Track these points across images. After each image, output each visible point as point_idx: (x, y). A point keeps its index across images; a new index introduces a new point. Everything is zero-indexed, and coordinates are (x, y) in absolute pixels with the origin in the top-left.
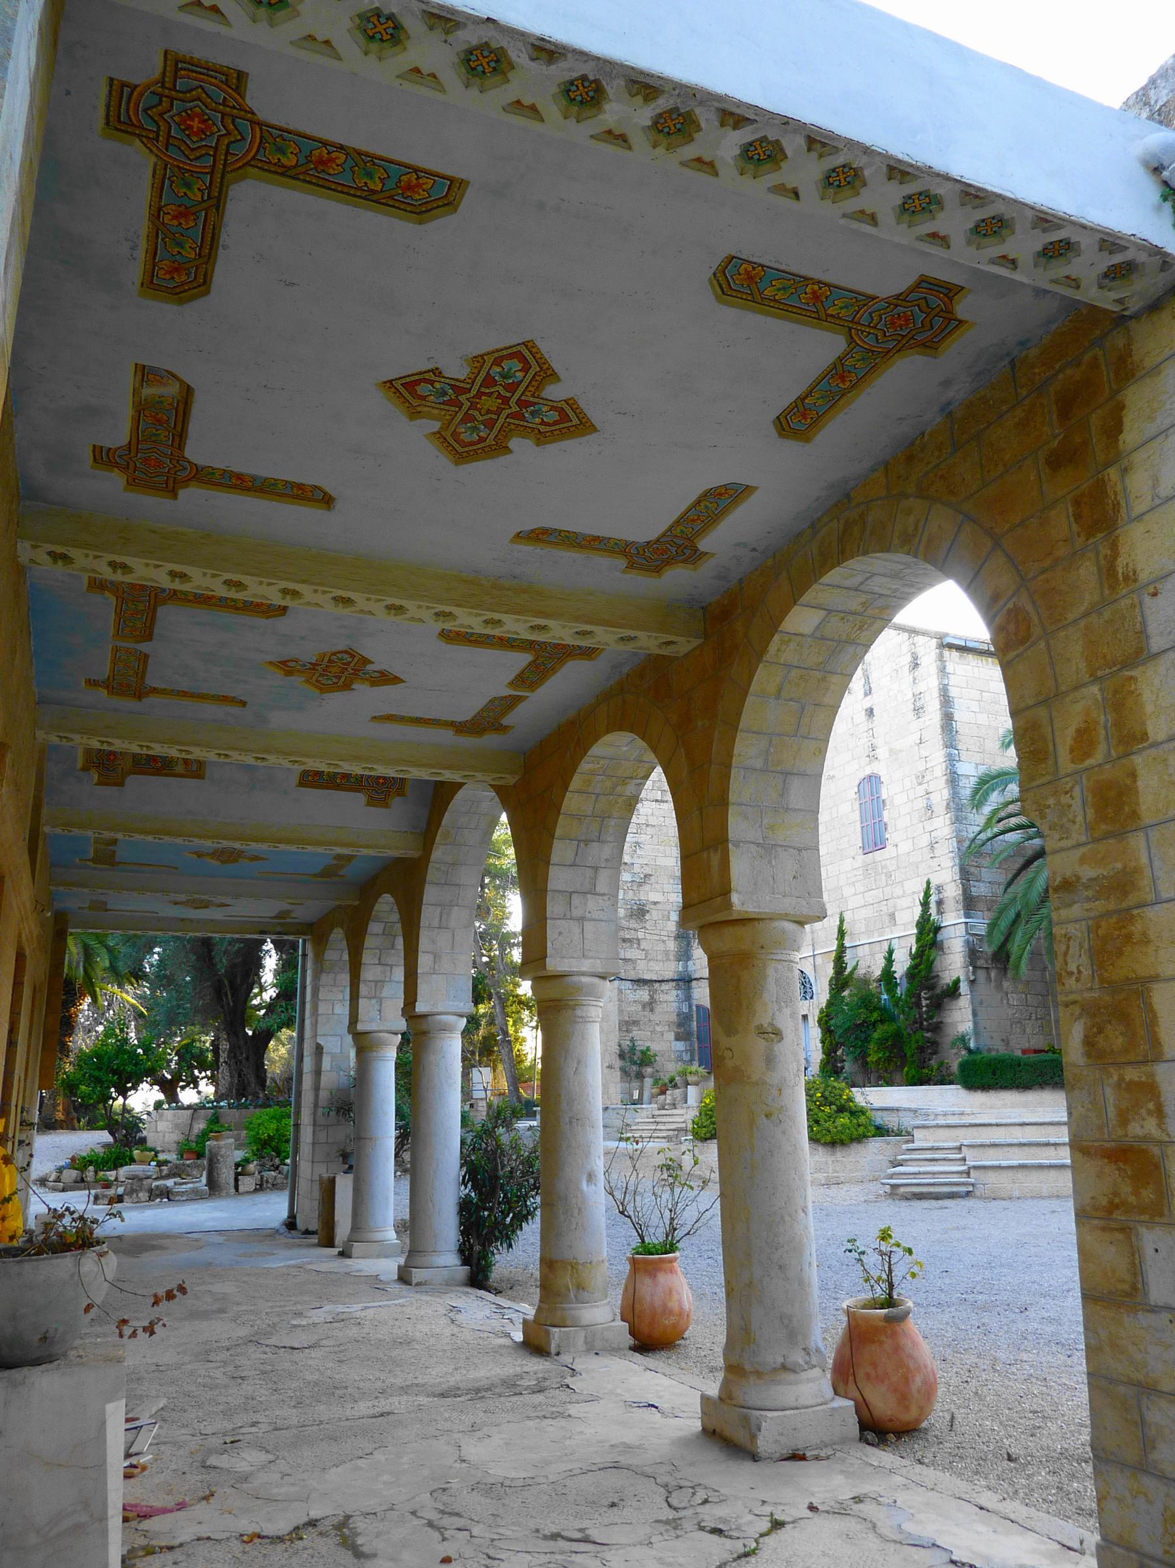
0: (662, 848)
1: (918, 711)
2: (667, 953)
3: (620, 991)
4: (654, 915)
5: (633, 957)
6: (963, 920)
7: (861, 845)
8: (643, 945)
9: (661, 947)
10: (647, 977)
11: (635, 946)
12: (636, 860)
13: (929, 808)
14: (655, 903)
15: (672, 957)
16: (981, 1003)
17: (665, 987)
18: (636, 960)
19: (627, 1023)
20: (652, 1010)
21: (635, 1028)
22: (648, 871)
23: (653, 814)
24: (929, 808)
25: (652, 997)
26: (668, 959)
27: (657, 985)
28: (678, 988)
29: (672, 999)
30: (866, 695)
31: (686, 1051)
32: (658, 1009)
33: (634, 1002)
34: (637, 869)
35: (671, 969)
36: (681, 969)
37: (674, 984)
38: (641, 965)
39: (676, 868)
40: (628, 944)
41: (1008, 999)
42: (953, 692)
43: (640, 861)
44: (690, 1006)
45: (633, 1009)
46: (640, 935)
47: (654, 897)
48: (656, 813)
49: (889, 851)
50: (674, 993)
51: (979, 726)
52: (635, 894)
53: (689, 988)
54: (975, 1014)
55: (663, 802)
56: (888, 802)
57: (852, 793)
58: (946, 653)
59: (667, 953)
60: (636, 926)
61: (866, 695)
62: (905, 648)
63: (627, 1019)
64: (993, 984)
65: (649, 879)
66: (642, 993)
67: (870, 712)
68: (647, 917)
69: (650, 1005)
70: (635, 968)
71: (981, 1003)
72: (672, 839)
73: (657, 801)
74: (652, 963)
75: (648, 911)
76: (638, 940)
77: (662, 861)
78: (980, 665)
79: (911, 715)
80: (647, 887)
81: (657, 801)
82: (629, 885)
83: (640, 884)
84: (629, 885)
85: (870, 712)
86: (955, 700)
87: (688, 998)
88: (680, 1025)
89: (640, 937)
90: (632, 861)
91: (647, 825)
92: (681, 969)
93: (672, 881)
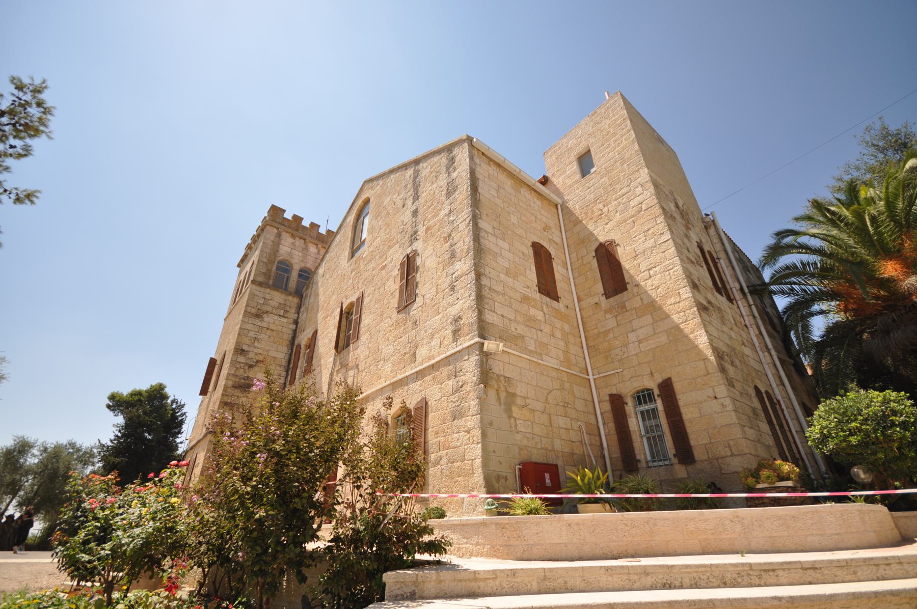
0: (276, 346)
1: (450, 191)
6: (477, 339)
7: (397, 306)
13: (453, 256)
16: (491, 424)
22: (261, 358)
23: (274, 323)
24: (453, 256)
34: (251, 355)
39: (284, 361)
41: (516, 425)
42: (479, 175)
43: (256, 350)
48: (277, 322)
49: (419, 300)
51: (496, 205)
52: (245, 372)
54: (484, 435)
55: (284, 317)
56: (421, 267)
57: (396, 272)
60: (240, 395)
64: (503, 407)
71: (491, 424)
73: (279, 315)
77: (273, 354)
78: (498, 170)
79: (444, 198)
80: (256, 369)
81: (279, 315)
82: (242, 365)
83: (251, 366)
85: (415, 213)
86: (480, 181)
90: (249, 349)
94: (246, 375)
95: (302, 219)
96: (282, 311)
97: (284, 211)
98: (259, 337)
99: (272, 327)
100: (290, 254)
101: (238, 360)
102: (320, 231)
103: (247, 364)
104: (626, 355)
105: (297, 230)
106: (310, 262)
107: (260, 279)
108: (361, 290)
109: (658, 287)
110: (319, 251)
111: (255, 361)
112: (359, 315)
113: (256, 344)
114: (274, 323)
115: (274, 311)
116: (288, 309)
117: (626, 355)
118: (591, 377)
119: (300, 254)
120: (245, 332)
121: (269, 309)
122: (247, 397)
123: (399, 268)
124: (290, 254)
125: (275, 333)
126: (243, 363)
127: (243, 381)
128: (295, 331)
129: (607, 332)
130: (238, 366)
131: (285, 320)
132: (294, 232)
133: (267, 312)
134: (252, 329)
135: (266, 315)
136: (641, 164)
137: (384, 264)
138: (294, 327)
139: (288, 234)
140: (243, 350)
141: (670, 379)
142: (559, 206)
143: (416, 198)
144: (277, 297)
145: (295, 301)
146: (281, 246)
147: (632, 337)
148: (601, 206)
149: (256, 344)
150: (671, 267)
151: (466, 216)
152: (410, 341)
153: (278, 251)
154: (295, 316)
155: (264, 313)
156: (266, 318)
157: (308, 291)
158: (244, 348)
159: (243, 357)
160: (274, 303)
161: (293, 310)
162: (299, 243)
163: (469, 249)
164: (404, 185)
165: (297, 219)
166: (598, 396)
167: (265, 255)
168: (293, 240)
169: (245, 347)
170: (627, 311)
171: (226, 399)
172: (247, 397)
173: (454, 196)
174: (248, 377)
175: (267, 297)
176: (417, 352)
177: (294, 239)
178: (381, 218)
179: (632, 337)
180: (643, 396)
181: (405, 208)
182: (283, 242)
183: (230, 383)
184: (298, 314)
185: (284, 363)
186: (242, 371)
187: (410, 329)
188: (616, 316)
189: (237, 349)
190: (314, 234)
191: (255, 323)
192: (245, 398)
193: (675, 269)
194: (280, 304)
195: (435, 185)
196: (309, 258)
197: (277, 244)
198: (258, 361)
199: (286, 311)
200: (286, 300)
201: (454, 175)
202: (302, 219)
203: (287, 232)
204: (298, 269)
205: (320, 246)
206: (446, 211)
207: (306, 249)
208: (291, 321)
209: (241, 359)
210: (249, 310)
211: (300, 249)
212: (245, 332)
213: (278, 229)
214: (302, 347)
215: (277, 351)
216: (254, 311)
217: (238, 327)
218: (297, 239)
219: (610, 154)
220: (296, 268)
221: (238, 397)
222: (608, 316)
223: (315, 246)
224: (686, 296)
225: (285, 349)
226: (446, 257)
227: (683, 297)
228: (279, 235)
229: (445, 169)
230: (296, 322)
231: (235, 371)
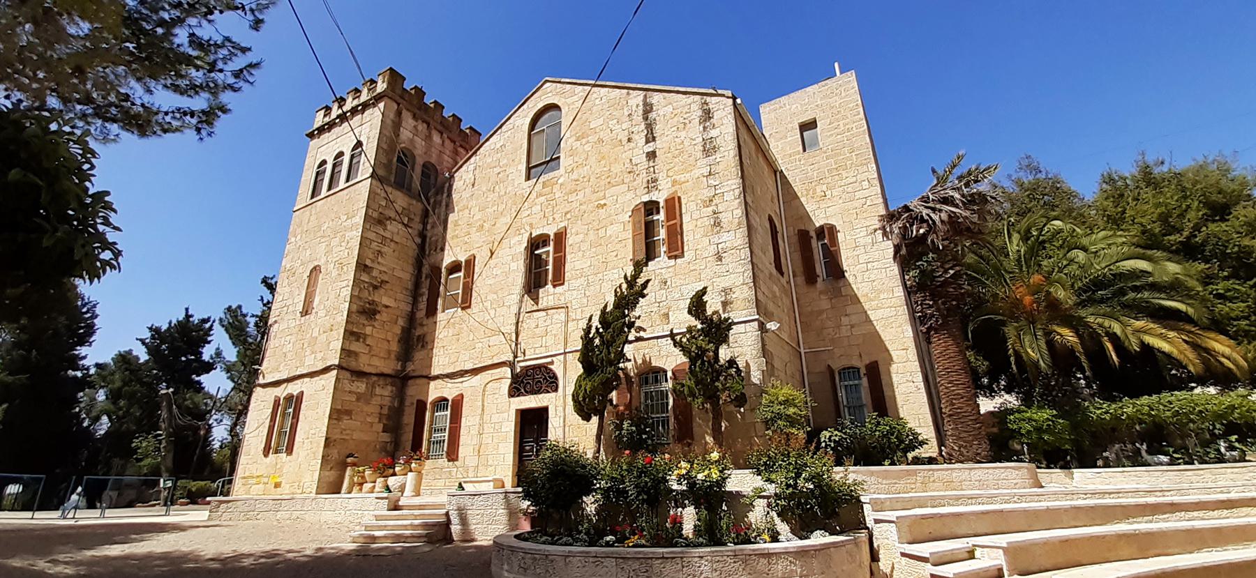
1: (709, 148)
2: (389, 352)
3: (337, 380)
4: (383, 317)
6: (757, 317)
9: (385, 344)
11: (361, 340)
12: (375, 265)
13: (717, 224)
14: (387, 307)
19: (338, 411)
21: (346, 417)
22: (385, 278)
29: (386, 394)
30: (647, 142)
31: (391, 442)
34: (375, 273)
35: (389, 366)
36: (399, 368)
44: (402, 402)
46: (368, 330)
47: (385, 301)
50: (389, 388)
52: (370, 294)
57: (626, 217)
60: (366, 322)
61: (647, 142)
62: (695, 107)
63: (340, 407)
66: (359, 384)
67: (652, 155)
75: (379, 312)
76: (365, 335)
79: (699, 154)
80: (382, 291)
82: (366, 285)
83: (375, 287)
85: (652, 155)
87: (401, 395)
88: (389, 417)
89: (367, 333)
91: (392, 240)
92: (399, 368)
94: (370, 298)
96: (407, 219)
98: (383, 250)
99: (396, 239)
100: (412, 141)
101: (362, 278)
103: (371, 284)
104: (838, 335)
105: (419, 109)
106: (434, 155)
108: (562, 225)
109: (874, 281)
110: (443, 142)
112: (563, 254)
113: (380, 259)
114: (398, 233)
116: (412, 216)
117: (838, 335)
118: (802, 351)
119: (423, 143)
121: (393, 214)
122: (374, 326)
123: (630, 214)
124: (412, 141)
126: (367, 282)
127: (367, 305)
128: (422, 247)
129: (821, 312)
132: (418, 112)
133: (390, 217)
135: (388, 222)
136: (870, 158)
137: (602, 202)
138: (418, 240)
139: (409, 114)
140: (366, 266)
141: (876, 362)
142: (778, 173)
143: (650, 138)
144: (401, 200)
145: (417, 207)
146: (401, 129)
147: (845, 320)
148: (824, 188)
149: (380, 259)
150: (888, 265)
151: (734, 187)
152: (658, 300)
154: (420, 227)
156: (393, 227)
157: (439, 198)
159: (366, 275)
161: (417, 219)
162: (422, 127)
163: (739, 224)
164: (627, 113)
166: (807, 368)
168: (415, 123)
169: (368, 262)
170: (842, 296)
171: (350, 327)
172: (374, 326)
173: (714, 157)
174: (374, 301)
176: (670, 313)
177: (417, 121)
178: (588, 142)
179: (845, 320)
180: (850, 372)
181: (632, 145)
182: (404, 124)
183: (355, 307)
184: (425, 224)
185: (410, 286)
186: (366, 294)
187: (658, 288)
188: (831, 299)
193: (892, 268)
194: (404, 208)
195: (683, 134)
196: (433, 150)
197: (397, 125)
198: (382, 282)
200: (410, 204)
201: (714, 133)
203: (408, 110)
204: (422, 163)
205: (445, 135)
206: (706, 171)
207: (429, 138)
209: (365, 277)
210: (370, 214)
213: (399, 104)
214: (443, 270)
216: (375, 215)
217: (357, 234)
218: (420, 122)
219: (839, 136)
220: (420, 161)
221: (364, 325)
222: (822, 297)
224: (899, 294)
225: (410, 269)
226: (707, 223)
227: (896, 295)
229: (697, 120)
230: (423, 235)
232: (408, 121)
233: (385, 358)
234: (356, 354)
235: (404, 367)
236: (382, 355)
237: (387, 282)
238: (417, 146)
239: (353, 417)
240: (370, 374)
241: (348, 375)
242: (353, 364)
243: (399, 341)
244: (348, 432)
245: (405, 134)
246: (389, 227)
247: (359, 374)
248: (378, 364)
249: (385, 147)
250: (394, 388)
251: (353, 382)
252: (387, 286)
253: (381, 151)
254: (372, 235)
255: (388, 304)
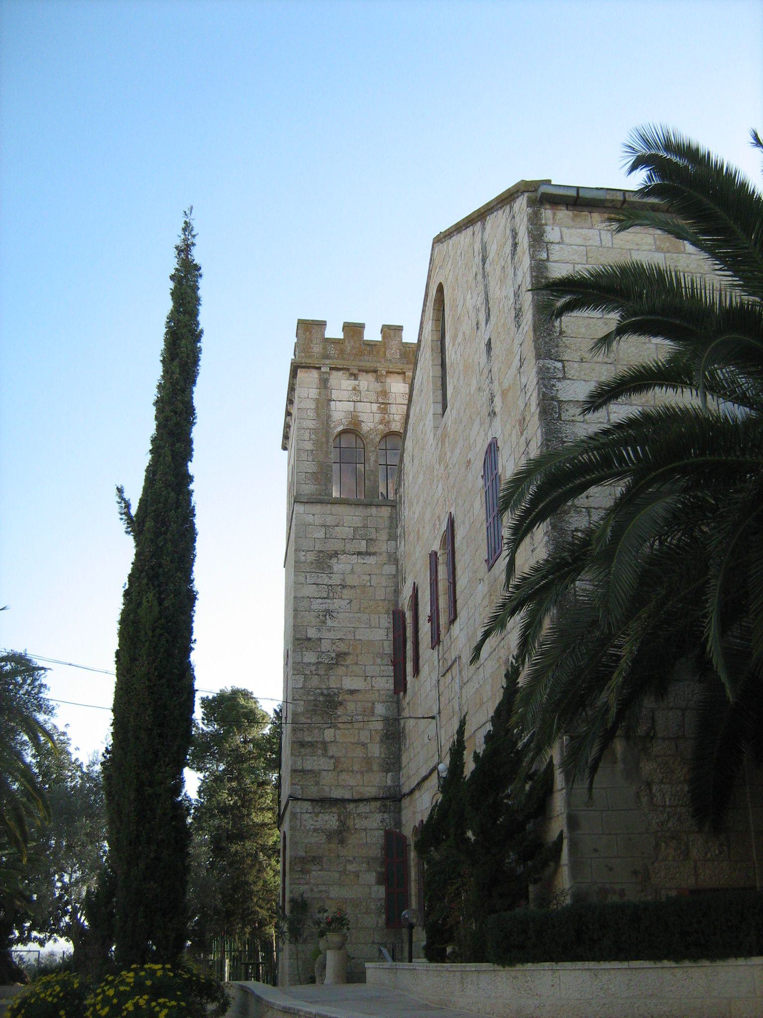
0: (365, 617)
2: (368, 761)
5: (316, 768)
8: (332, 750)
9: (359, 752)
10: (336, 794)
12: (325, 635)
14: (352, 692)
15: (375, 767)
17: (363, 808)
18: (320, 772)
20: (342, 842)
21: (314, 868)
22: (343, 647)
23: (352, 572)
25: (343, 823)
26: (370, 770)
27: (351, 807)
28: (384, 809)
29: (375, 825)
32: (352, 840)
33: (315, 830)
34: (325, 646)
36: (389, 783)
37: (378, 804)
38: (327, 779)
39: (386, 644)
40: (308, 750)
43: (332, 635)
45: (313, 840)
46: (329, 734)
47: (349, 683)
50: (378, 817)
53: (399, 811)
58: (547, 213)
59: (368, 761)
63: (302, 853)
65: (345, 660)
66: (327, 817)
68: (340, 712)
69: (340, 835)
70: (317, 783)
72: (380, 603)
73: (359, 553)
74: (344, 776)
75: (341, 704)
76: (325, 744)
77: (364, 634)
80: (341, 670)
81: (359, 553)
82: (313, 668)
83: (330, 667)
84: (313, 668)
89: (327, 739)
90: (319, 636)
92: (389, 783)
93: (379, 661)
95: (361, 326)
96: (364, 543)
97: (322, 324)
101: (306, 660)
102: (404, 341)
107: (308, 489)
111: (333, 655)
115: (350, 547)
120: (305, 603)
121: (337, 545)
125: (358, 591)
130: (308, 673)
131: (372, 560)
134: (316, 595)
135: (334, 560)
139: (340, 373)
144: (351, 517)
149: (329, 622)
153: (329, 417)
155: (331, 557)
156: (341, 565)
158: (309, 636)
160: (345, 531)
161: (383, 535)
162: (366, 382)
165: (354, 330)
167: (307, 436)
168: (352, 383)
169: (312, 633)
175: (330, 520)
177: (356, 379)
185: (388, 648)
189: (298, 639)
190: (393, 352)
191: (320, 581)
192: (333, 730)
194: (356, 529)
196: (393, 409)
197: (324, 402)
198: (341, 656)
199: (370, 541)
202: (361, 326)
208: (384, 558)
209: (310, 657)
211: (373, 397)
212: (305, 603)
215: (370, 627)
223: (400, 378)
228: (324, 383)
231: (305, 681)
232: (341, 384)
233: (362, 773)
234: (314, 774)
235: (397, 778)
236: (356, 768)
237: (346, 654)
238: (363, 417)
239: (325, 866)
240: (343, 801)
241: (307, 806)
242: (313, 791)
243: (382, 741)
244: (323, 888)
245: (340, 411)
246: (336, 568)
247: (324, 802)
248: (352, 782)
249: (309, 446)
250: (386, 816)
251: (317, 815)
252: (349, 660)
253: (304, 456)
254: (310, 591)
255: (353, 688)
